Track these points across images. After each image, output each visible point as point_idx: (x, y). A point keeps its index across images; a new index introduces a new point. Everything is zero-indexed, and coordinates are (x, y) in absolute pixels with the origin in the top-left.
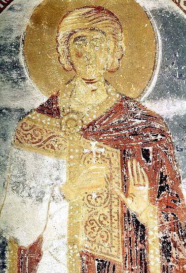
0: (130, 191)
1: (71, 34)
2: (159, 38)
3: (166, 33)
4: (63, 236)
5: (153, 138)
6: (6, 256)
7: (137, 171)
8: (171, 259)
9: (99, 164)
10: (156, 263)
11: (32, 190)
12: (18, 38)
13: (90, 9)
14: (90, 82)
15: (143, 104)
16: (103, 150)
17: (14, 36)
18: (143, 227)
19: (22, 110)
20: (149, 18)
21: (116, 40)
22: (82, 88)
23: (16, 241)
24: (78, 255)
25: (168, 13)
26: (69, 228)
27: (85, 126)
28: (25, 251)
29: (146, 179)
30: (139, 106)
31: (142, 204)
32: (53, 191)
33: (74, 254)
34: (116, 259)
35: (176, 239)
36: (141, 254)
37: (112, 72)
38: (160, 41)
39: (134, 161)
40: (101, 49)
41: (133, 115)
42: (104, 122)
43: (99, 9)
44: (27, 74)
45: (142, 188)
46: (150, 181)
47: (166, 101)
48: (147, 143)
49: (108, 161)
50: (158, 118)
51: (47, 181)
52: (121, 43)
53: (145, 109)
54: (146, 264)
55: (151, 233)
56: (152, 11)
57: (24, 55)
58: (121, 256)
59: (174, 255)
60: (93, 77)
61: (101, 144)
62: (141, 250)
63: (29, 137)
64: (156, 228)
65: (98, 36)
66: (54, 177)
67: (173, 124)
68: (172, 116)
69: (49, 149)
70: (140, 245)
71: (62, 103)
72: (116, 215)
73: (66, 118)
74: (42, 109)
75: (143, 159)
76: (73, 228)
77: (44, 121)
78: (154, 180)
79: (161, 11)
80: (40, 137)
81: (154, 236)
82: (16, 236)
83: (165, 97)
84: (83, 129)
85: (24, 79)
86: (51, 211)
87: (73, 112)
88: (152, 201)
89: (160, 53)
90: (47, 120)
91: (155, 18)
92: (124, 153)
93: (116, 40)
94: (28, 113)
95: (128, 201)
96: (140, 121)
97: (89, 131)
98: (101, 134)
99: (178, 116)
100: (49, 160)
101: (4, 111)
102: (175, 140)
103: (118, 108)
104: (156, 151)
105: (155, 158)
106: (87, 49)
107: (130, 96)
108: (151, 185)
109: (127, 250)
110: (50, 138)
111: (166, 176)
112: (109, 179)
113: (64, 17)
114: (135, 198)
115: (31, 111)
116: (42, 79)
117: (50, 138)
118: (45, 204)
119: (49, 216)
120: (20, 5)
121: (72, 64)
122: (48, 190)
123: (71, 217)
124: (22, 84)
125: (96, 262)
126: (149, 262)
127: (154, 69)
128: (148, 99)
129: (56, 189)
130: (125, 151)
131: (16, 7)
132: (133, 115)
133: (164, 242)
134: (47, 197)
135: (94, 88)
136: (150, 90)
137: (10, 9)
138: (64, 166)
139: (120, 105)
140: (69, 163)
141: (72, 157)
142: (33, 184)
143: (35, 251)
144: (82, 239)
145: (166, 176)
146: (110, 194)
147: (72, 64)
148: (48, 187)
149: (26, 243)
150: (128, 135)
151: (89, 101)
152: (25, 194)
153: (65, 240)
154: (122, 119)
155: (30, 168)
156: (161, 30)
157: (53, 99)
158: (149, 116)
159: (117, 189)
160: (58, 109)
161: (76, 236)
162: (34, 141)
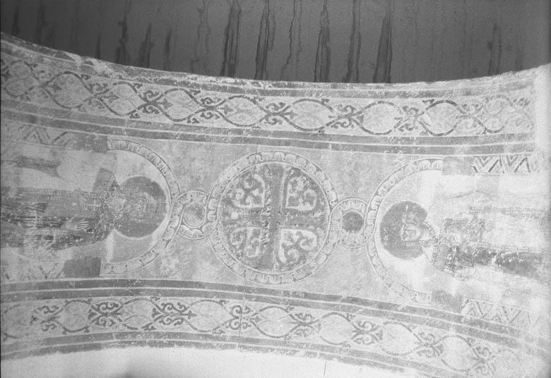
23: (59, 165)
30: (112, 228)
31: (70, 226)
50: (105, 237)
74: (114, 182)
81: (56, 233)
95: (71, 221)
104: (92, 235)
105: (88, 234)
116: (128, 183)
143: (56, 174)
151: (118, 203)
158: (107, 233)
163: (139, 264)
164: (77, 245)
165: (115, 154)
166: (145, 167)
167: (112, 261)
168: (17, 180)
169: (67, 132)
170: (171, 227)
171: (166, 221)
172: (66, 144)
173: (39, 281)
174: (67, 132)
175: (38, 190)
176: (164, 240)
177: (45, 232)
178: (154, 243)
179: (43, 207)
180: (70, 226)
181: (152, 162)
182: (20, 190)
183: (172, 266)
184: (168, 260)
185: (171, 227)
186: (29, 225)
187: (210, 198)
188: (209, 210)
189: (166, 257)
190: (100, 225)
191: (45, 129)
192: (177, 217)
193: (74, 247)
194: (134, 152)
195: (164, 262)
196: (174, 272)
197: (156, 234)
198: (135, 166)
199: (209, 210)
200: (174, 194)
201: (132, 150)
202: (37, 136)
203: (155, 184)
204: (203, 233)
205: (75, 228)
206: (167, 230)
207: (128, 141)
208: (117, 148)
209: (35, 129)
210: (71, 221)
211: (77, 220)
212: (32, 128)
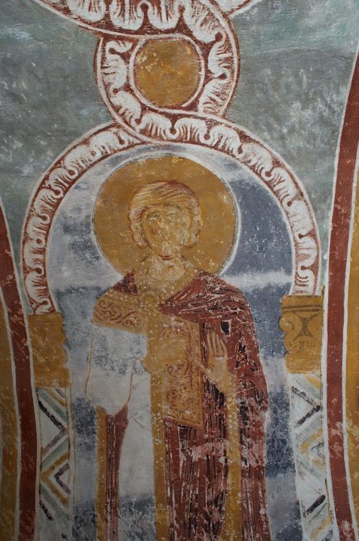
0: (210, 362)
1: (143, 211)
2: (239, 210)
3: (245, 205)
4: (147, 406)
5: (232, 311)
6: (95, 423)
7: (216, 342)
8: (248, 422)
9: (179, 336)
10: (234, 426)
11: (115, 364)
12: (88, 217)
13: (164, 183)
14: (167, 258)
15: (222, 279)
16: (182, 324)
17: (83, 215)
18: (222, 395)
19: (98, 288)
20: (227, 190)
21: (192, 215)
22: (158, 265)
23: (103, 410)
24: (162, 421)
25: (248, 184)
26: (152, 397)
27: (163, 302)
28: (112, 419)
29: (225, 349)
30: (218, 281)
31: (221, 374)
32: (135, 364)
33: (158, 421)
34: (197, 425)
35: (253, 404)
36: (220, 419)
37: (190, 247)
38: (239, 214)
39: (213, 334)
40: (177, 224)
41: (212, 290)
42: (182, 298)
43: (173, 183)
44: (100, 254)
45: (221, 358)
46: (228, 352)
47: (245, 275)
48: (226, 317)
49: (187, 335)
51: (129, 355)
52: (198, 218)
53: (224, 284)
54: (224, 427)
55: (229, 400)
56: (231, 183)
57: (95, 233)
58: (202, 422)
59: (251, 418)
60: (170, 253)
61: (180, 318)
62: (220, 415)
63: (108, 314)
64: (235, 395)
65: (173, 212)
66: (135, 351)
67: (252, 297)
68: (251, 289)
69: (129, 324)
70: (220, 411)
71: (139, 280)
72: (196, 385)
73: (143, 295)
74: (118, 287)
75: (222, 331)
76: (156, 399)
77: (121, 298)
78: (233, 350)
79: (240, 182)
80: (118, 314)
81: (232, 402)
82: (103, 406)
83: (245, 271)
84: (161, 305)
85: (98, 258)
86: (134, 383)
87: (149, 289)
88: (231, 370)
89: (240, 227)
90: (124, 297)
91: (234, 190)
92: (204, 327)
93: (192, 215)
94: (105, 291)
96: (219, 296)
97: (169, 307)
98: (180, 309)
99: (257, 290)
100: (127, 335)
101: (81, 289)
102: (254, 313)
103: (197, 284)
104: (235, 323)
106: (162, 225)
107: (209, 271)
108: (229, 356)
109: (207, 416)
110: (129, 314)
111: (245, 347)
112: (189, 351)
113: (136, 193)
114: (214, 369)
115: (108, 289)
117: (129, 314)
118: (128, 376)
119: (132, 388)
120: (86, 183)
121: (146, 241)
122: (130, 363)
123: (153, 388)
124: (96, 263)
125: (178, 427)
126: (227, 426)
127: (233, 243)
128: (228, 273)
129: (138, 361)
130: (204, 324)
131: (83, 186)
132: (212, 290)
133: (242, 407)
134: (129, 370)
135: (171, 264)
136: (229, 264)
137: (77, 187)
138: (144, 341)
139: (199, 280)
140: (149, 337)
141: (151, 332)
142: (115, 358)
144: (165, 407)
145: (245, 347)
146: (190, 365)
147: (146, 241)
148: (130, 360)
149: (112, 411)
150: (206, 310)
151: (167, 275)
152: (108, 367)
153: (149, 409)
154: (200, 294)
155: (111, 343)
156: (240, 204)
157: (128, 278)
158: (229, 290)
159: (197, 362)
160: (135, 286)
161: (159, 405)
162: (114, 317)
163: (299, 208)
164: (256, 351)
165: (59, 295)
166: (71, 223)
167: (289, 272)
168: (142, 505)
169: (40, 403)
170: (207, 137)
171: (193, 153)
172: (61, 403)
173: (325, 421)
174: (40, 403)
175: (157, 449)
176: (240, 151)
177: (233, 423)
178: (247, 173)
179: (187, 432)
180: (221, 374)
181: (56, 206)
182: (163, 500)
183: (308, 113)
184: (292, 130)
185: (207, 137)
186: (222, 460)
187: (109, 26)
188: (146, 27)
189: (282, 138)
190: (215, 308)
191: (43, 451)
192: (179, 123)
193: (260, 355)
194: (42, 251)
195: (295, 143)
196: (326, 113)
197: (226, 176)
198: (73, 246)
199: (146, 27)
200: (121, 142)
201: (40, 257)
202: (57, 470)
203: (104, 197)
204: (219, 37)
205: (223, 360)
206: (215, 147)
207: (26, 270)
208: (46, 290)
209: (45, 476)
210: (209, 371)
211: (205, 355)
212: (45, 486)
